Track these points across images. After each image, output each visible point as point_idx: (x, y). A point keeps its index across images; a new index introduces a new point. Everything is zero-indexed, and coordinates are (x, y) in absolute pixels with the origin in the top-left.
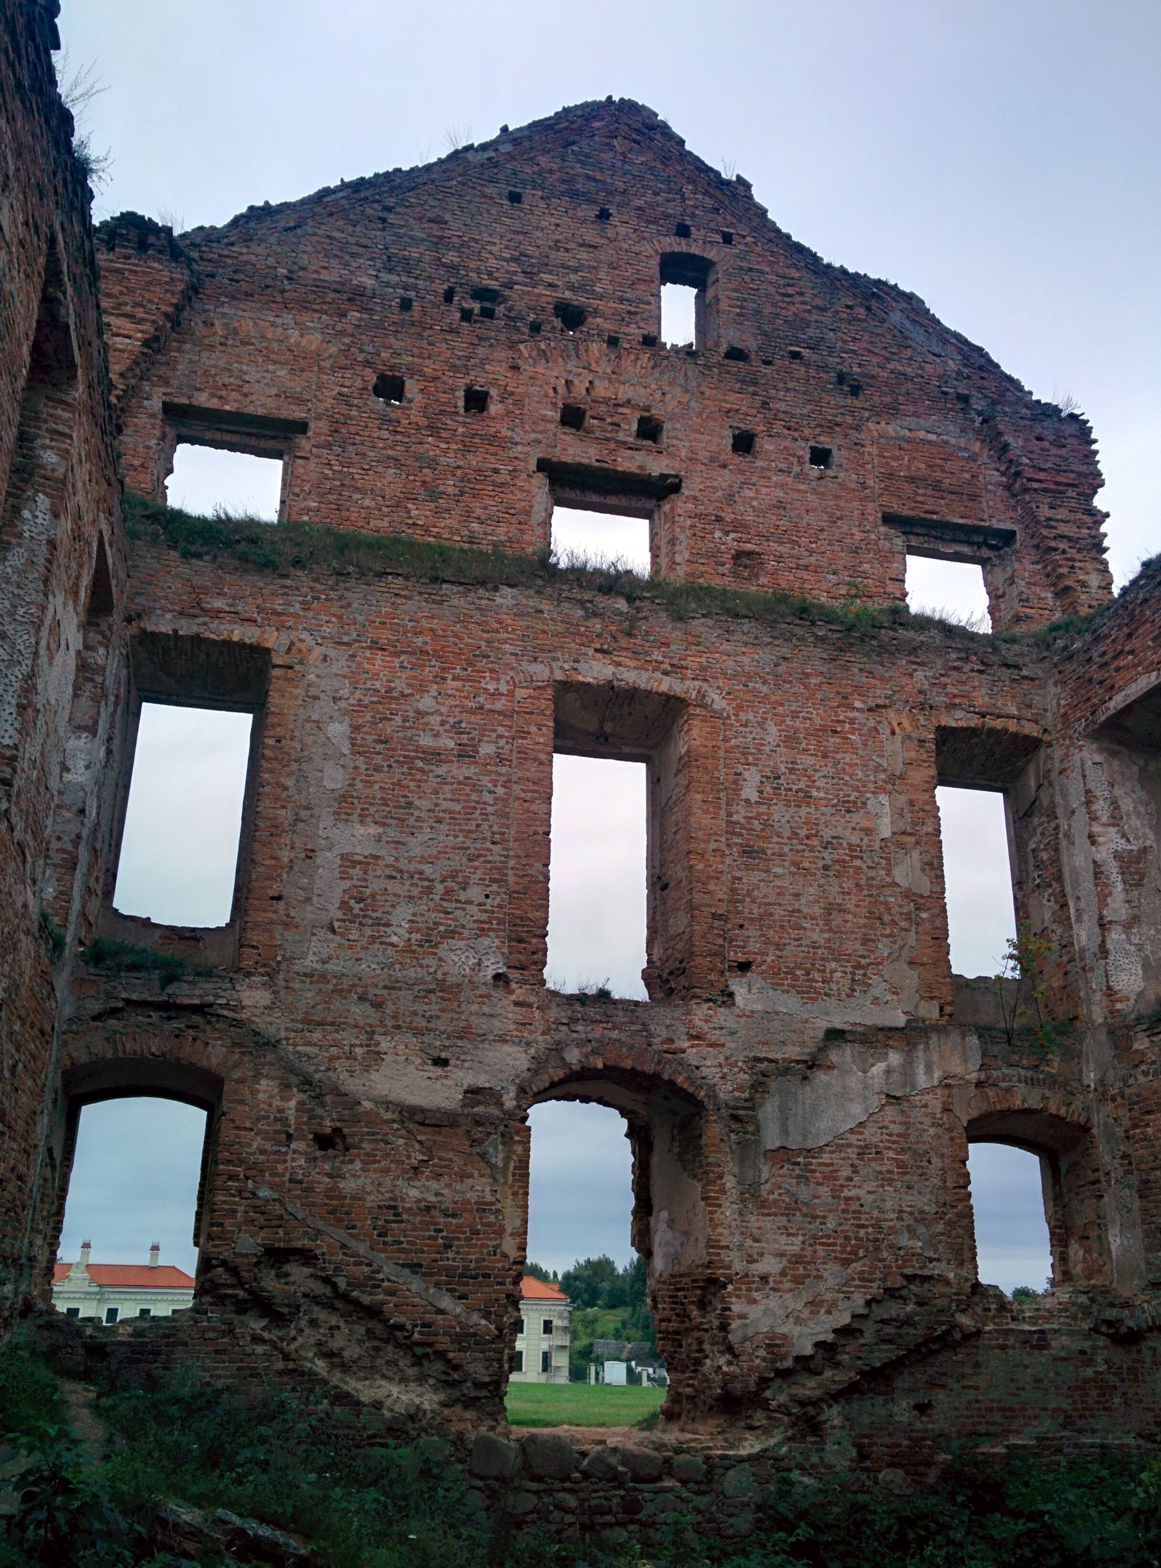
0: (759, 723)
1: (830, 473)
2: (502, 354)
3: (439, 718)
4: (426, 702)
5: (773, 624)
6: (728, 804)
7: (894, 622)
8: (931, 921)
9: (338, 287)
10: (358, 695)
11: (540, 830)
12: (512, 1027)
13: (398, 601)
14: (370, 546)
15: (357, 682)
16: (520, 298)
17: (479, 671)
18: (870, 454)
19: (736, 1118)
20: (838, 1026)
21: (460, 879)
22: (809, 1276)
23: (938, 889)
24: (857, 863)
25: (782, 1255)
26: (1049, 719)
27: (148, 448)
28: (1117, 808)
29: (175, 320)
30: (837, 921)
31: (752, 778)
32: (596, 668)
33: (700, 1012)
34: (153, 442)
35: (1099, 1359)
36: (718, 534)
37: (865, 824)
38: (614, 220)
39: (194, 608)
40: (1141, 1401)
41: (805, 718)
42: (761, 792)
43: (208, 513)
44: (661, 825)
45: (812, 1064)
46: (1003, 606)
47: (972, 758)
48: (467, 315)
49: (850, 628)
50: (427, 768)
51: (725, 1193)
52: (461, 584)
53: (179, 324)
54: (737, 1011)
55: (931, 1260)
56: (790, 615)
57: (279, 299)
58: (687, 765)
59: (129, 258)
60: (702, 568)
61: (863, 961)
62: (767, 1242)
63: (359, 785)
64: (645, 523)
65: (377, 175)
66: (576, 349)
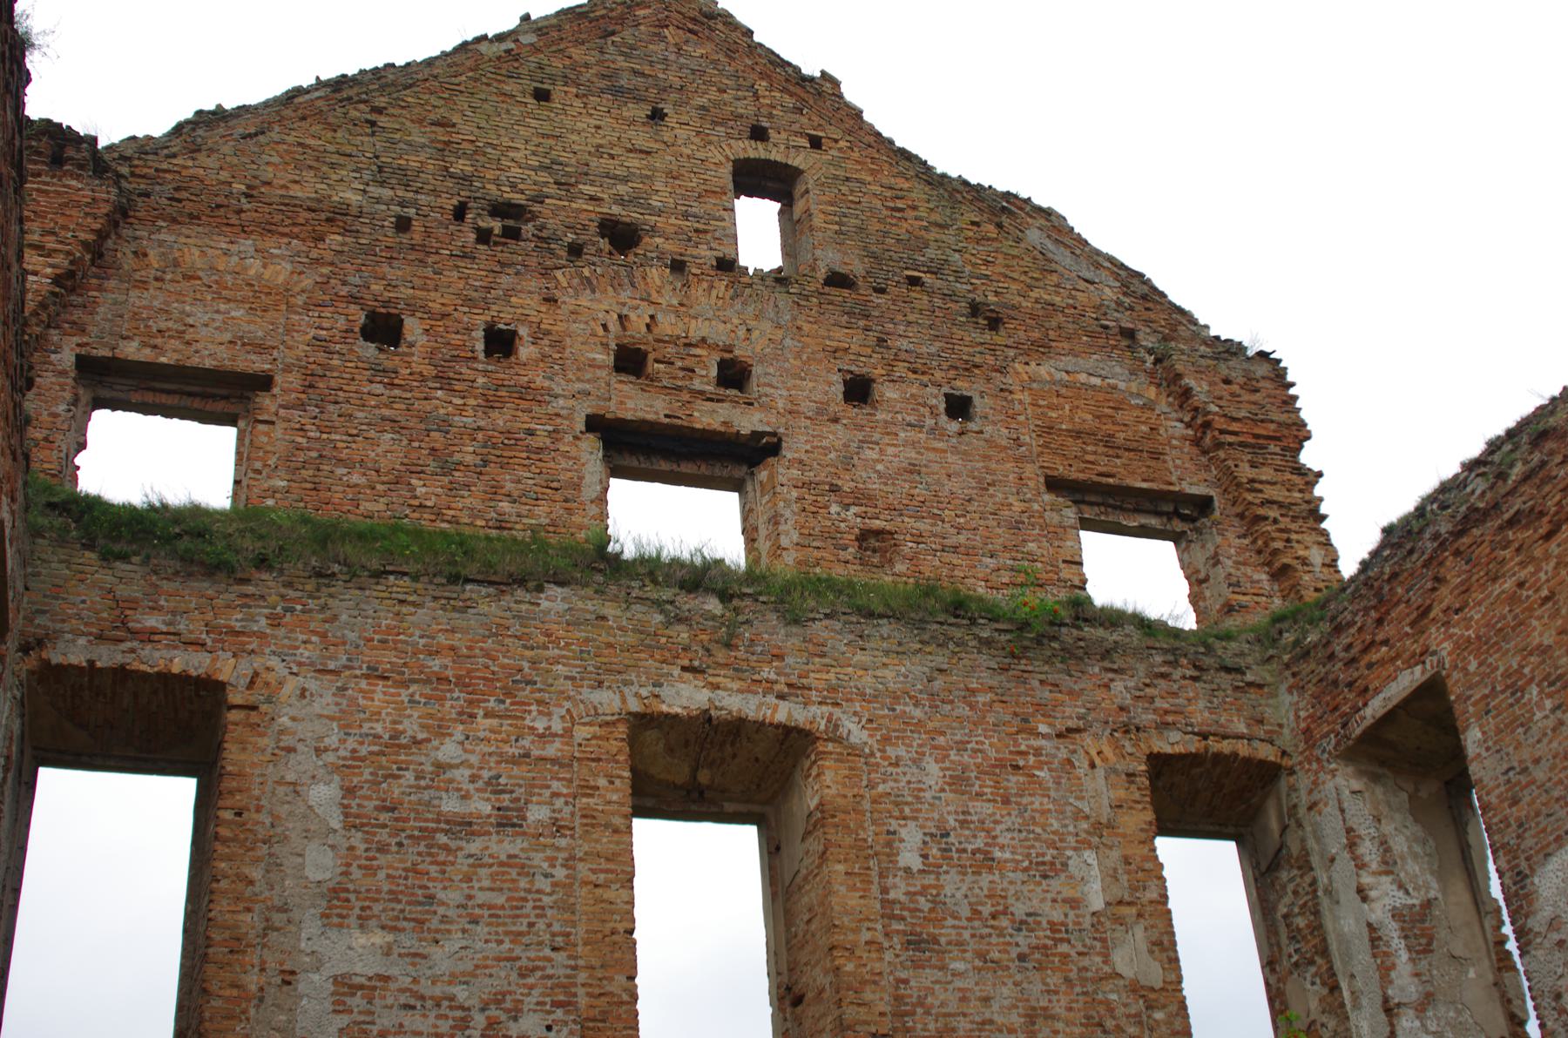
0: (914, 761)
1: (972, 426)
2: (533, 284)
3: (467, 772)
4: (449, 750)
5: (920, 625)
6: (881, 876)
7: (1077, 618)
8: (1169, 1023)
9: (314, 205)
10: (351, 743)
11: (621, 927)
13: (405, 609)
14: (361, 536)
15: (349, 726)
16: (554, 215)
17: (524, 704)
18: (1021, 402)
21: (508, 1005)
23: (1173, 977)
24: (1063, 948)
26: (1286, 738)
27: (55, 415)
28: (1388, 850)
29: (96, 251)
31: (911, 837)
32: (685, 693)
34: (62, 408)
36: (834, 508)
37: (1067, 893)
38: (671, 121)
39: (120, 629)
41: (975, 751)
42: (925, 857)
43: (137, 499)
44: (787, 912)
46: (1208, 594)
47: (1202, 793)
48: (484, 236)
49: (1024, 626)
50: (453, 844)
52: (491, 583)
53: (101, 255)
56: (943, 613)
57: (234, 221)
58: (820, 823)
59: (39, 175)
60: (816, 553)
63: (356, 873)
64: (733, 497)
65: (362, 72)
66: (631, 276)
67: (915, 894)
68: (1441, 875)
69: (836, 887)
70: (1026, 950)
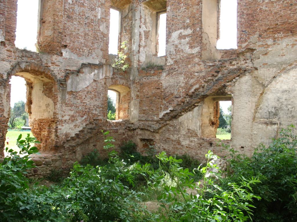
12: (6, 57)
19: (62, 84)
20: (85, 63)
22: (75, 120)
25: (69, 115)
28: (146, 21)
30: (87, 38)
33: (55, 57)
35: (126, 134)
37: (95, 14)
45: (79, 72)
51: (58, 101)
54: (63, 58)
55: (99, 116)
61: (91, 48)
62: (66, 112)
67: (70, 8)
68: (152, 27)
69: (57, 3)
70: (86, 23)
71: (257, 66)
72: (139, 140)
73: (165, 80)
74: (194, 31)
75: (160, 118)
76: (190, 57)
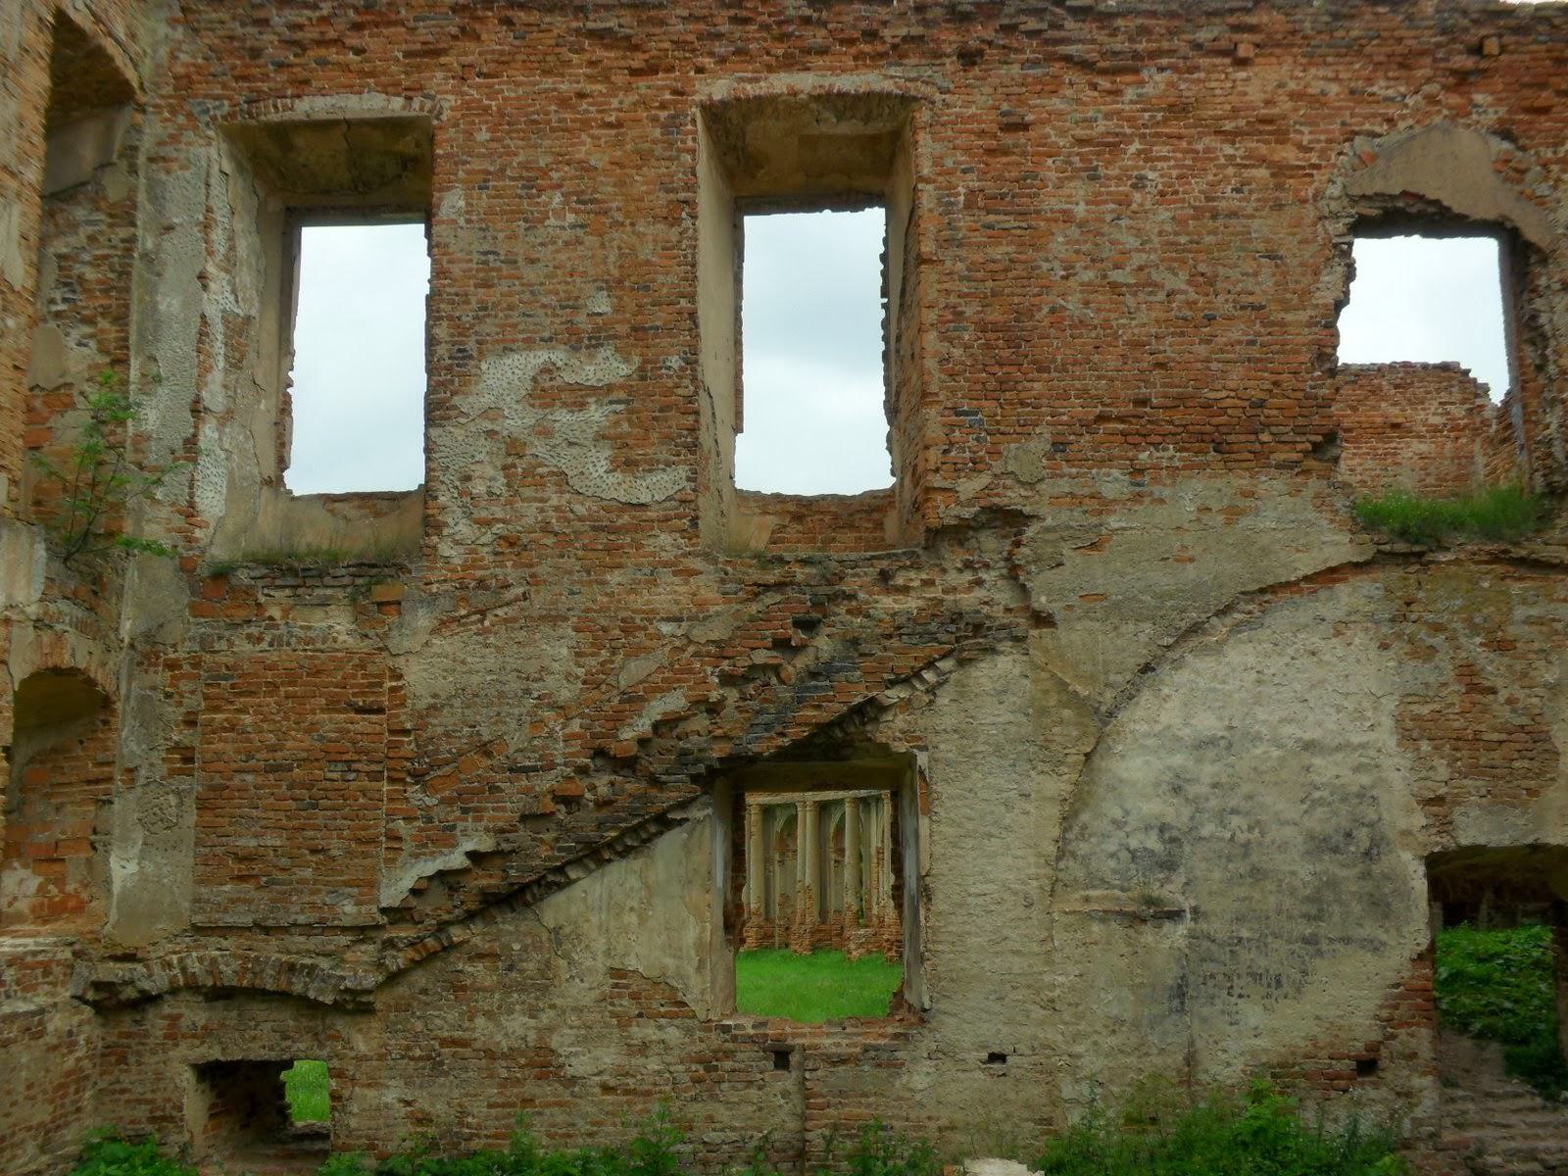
40: (123, 1091)
71: (1055, 608)
72: (187, 1078)
73: (430, 661)
74: (641, 369)
75: (384, 911)
76: (620, 522)
